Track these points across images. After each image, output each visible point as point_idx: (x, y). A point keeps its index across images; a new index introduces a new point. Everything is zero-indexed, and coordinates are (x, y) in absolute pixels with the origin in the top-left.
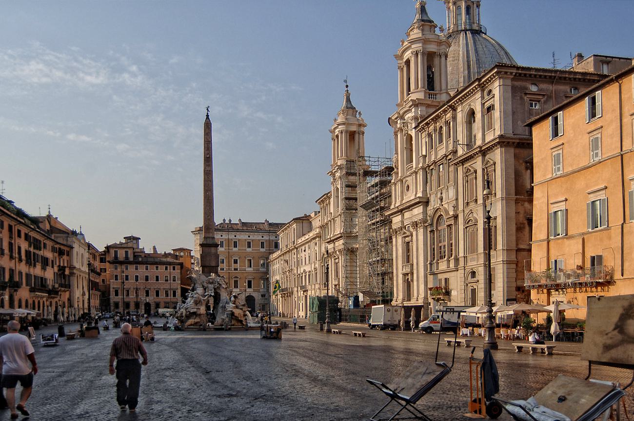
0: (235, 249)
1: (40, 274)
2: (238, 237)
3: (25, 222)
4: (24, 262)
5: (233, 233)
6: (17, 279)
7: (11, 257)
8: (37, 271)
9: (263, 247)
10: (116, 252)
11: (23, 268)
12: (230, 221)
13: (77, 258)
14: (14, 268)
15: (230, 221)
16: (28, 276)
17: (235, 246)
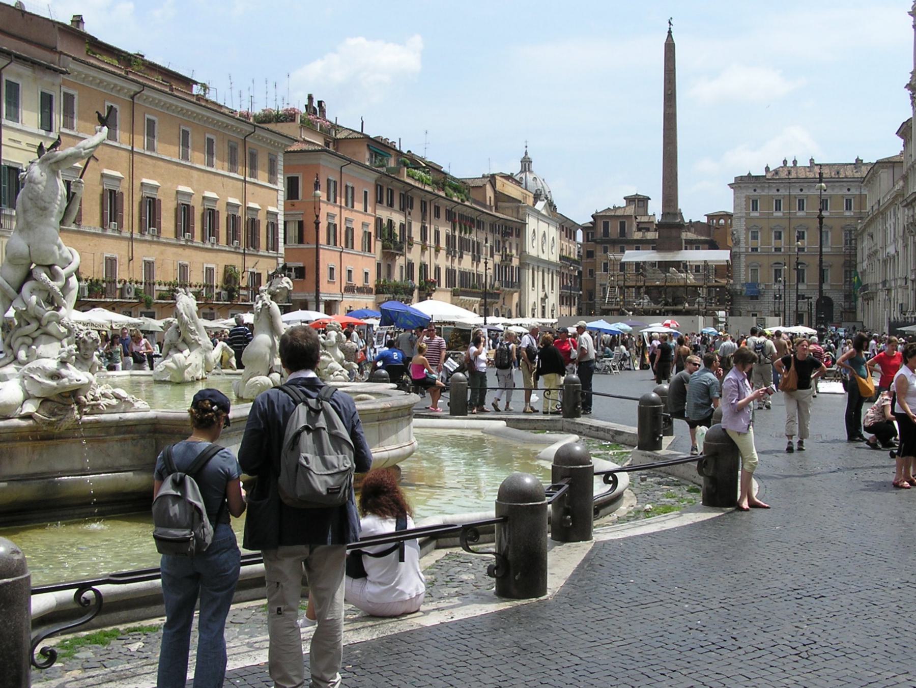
0: (800, 214)
1: (470, 268)
2: (805, 192)
3: (446, 194)
4: (443, 253)
5: (797, 185)
6: (431, 276)
7: (424, 249)
8: (466, 263)
9: (849, 207)
10: (606, 225)
11: (443, 261)
12: (795, 162)
13: (533, 240)
14: (428, 263)
15: (795, 162)
16: (450, 272)
17: (801, 208)
